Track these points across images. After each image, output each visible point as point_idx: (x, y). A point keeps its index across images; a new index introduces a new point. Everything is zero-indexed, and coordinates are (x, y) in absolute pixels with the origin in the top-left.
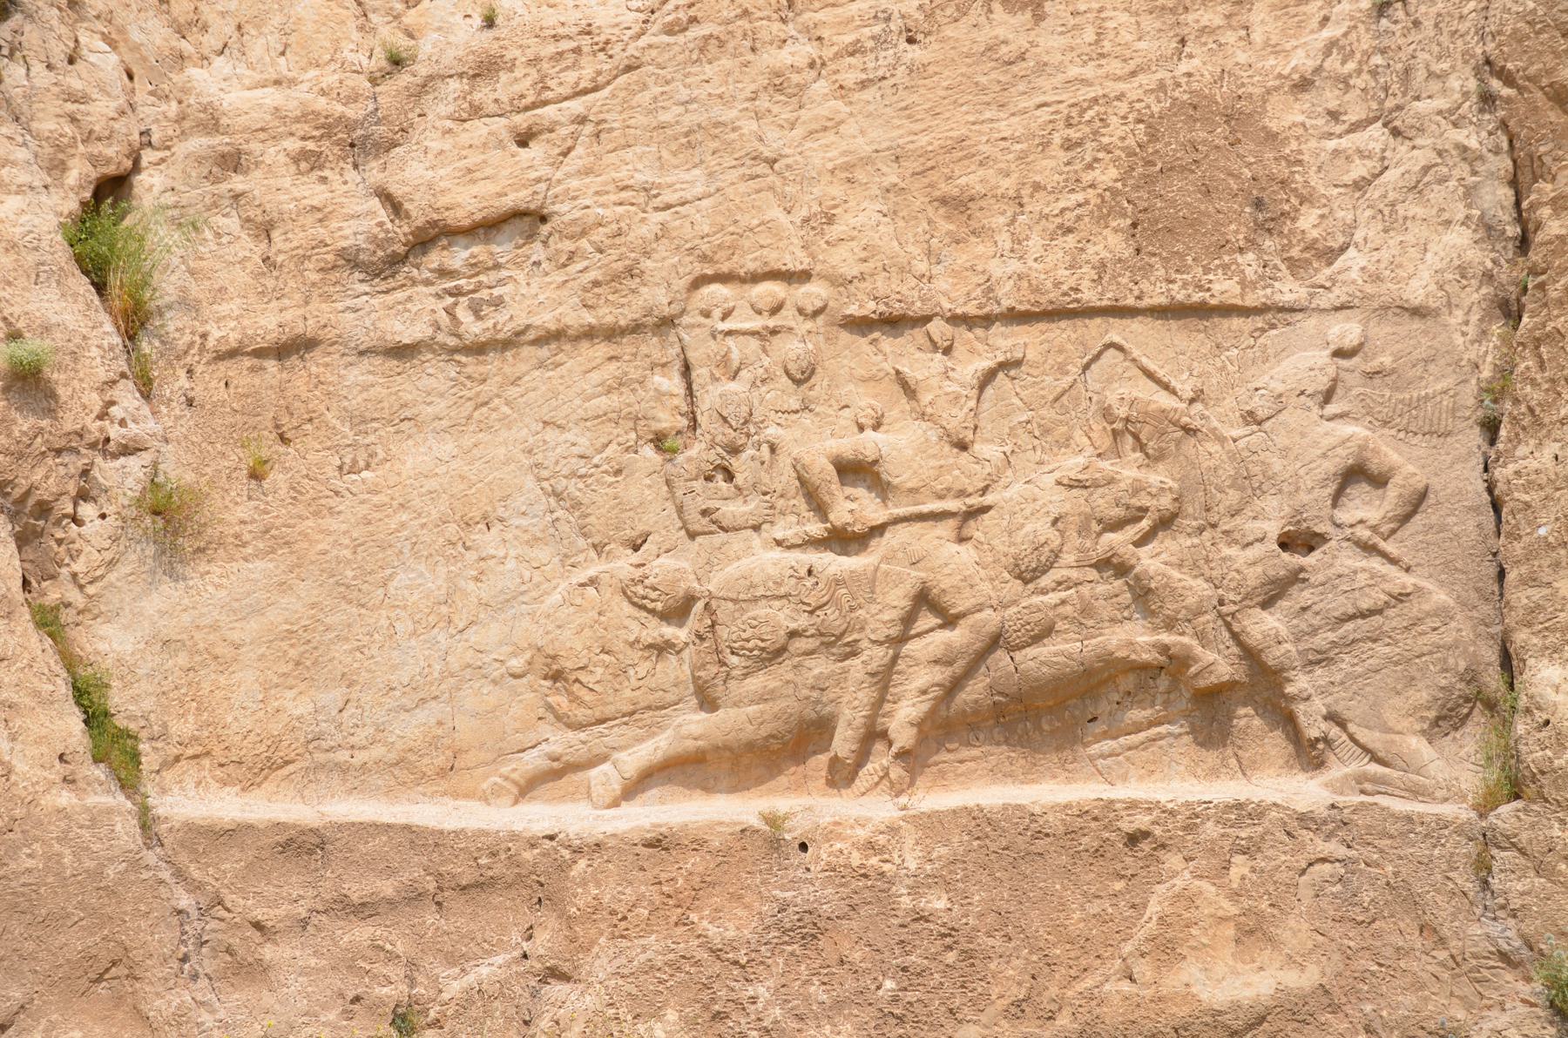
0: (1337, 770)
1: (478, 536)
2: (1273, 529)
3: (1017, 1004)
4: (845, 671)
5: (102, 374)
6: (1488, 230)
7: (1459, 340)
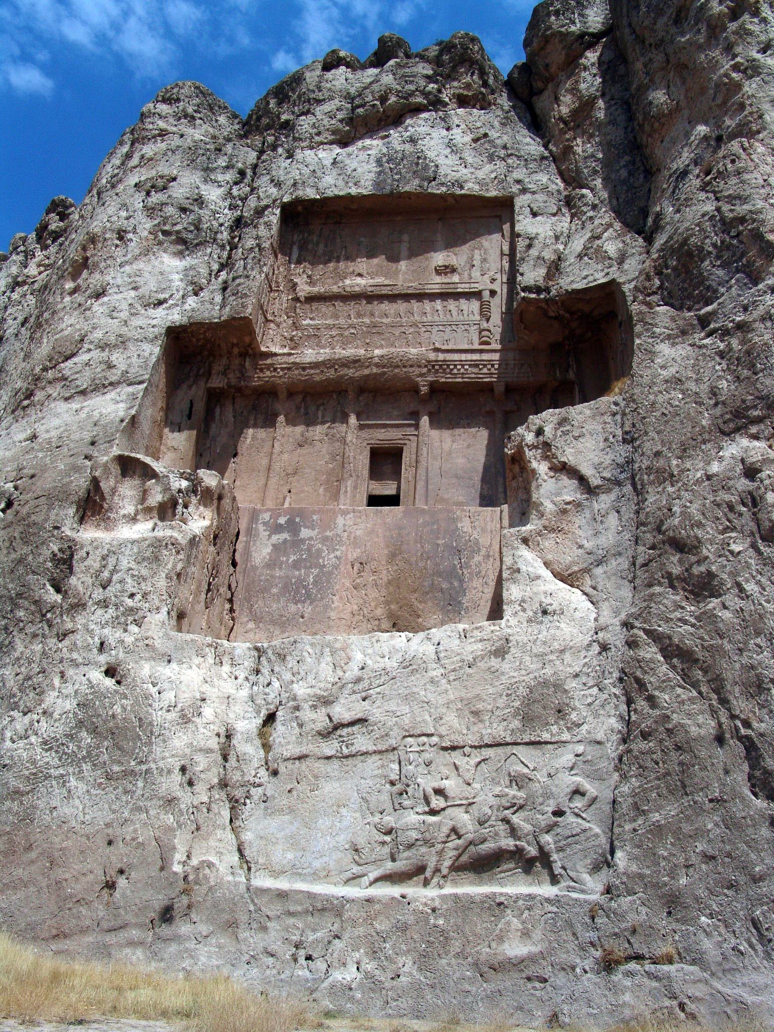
0: (563, 884)
2: (550, 809)
3: (458, 953)
5: (256, 766)
6: (621, 717)
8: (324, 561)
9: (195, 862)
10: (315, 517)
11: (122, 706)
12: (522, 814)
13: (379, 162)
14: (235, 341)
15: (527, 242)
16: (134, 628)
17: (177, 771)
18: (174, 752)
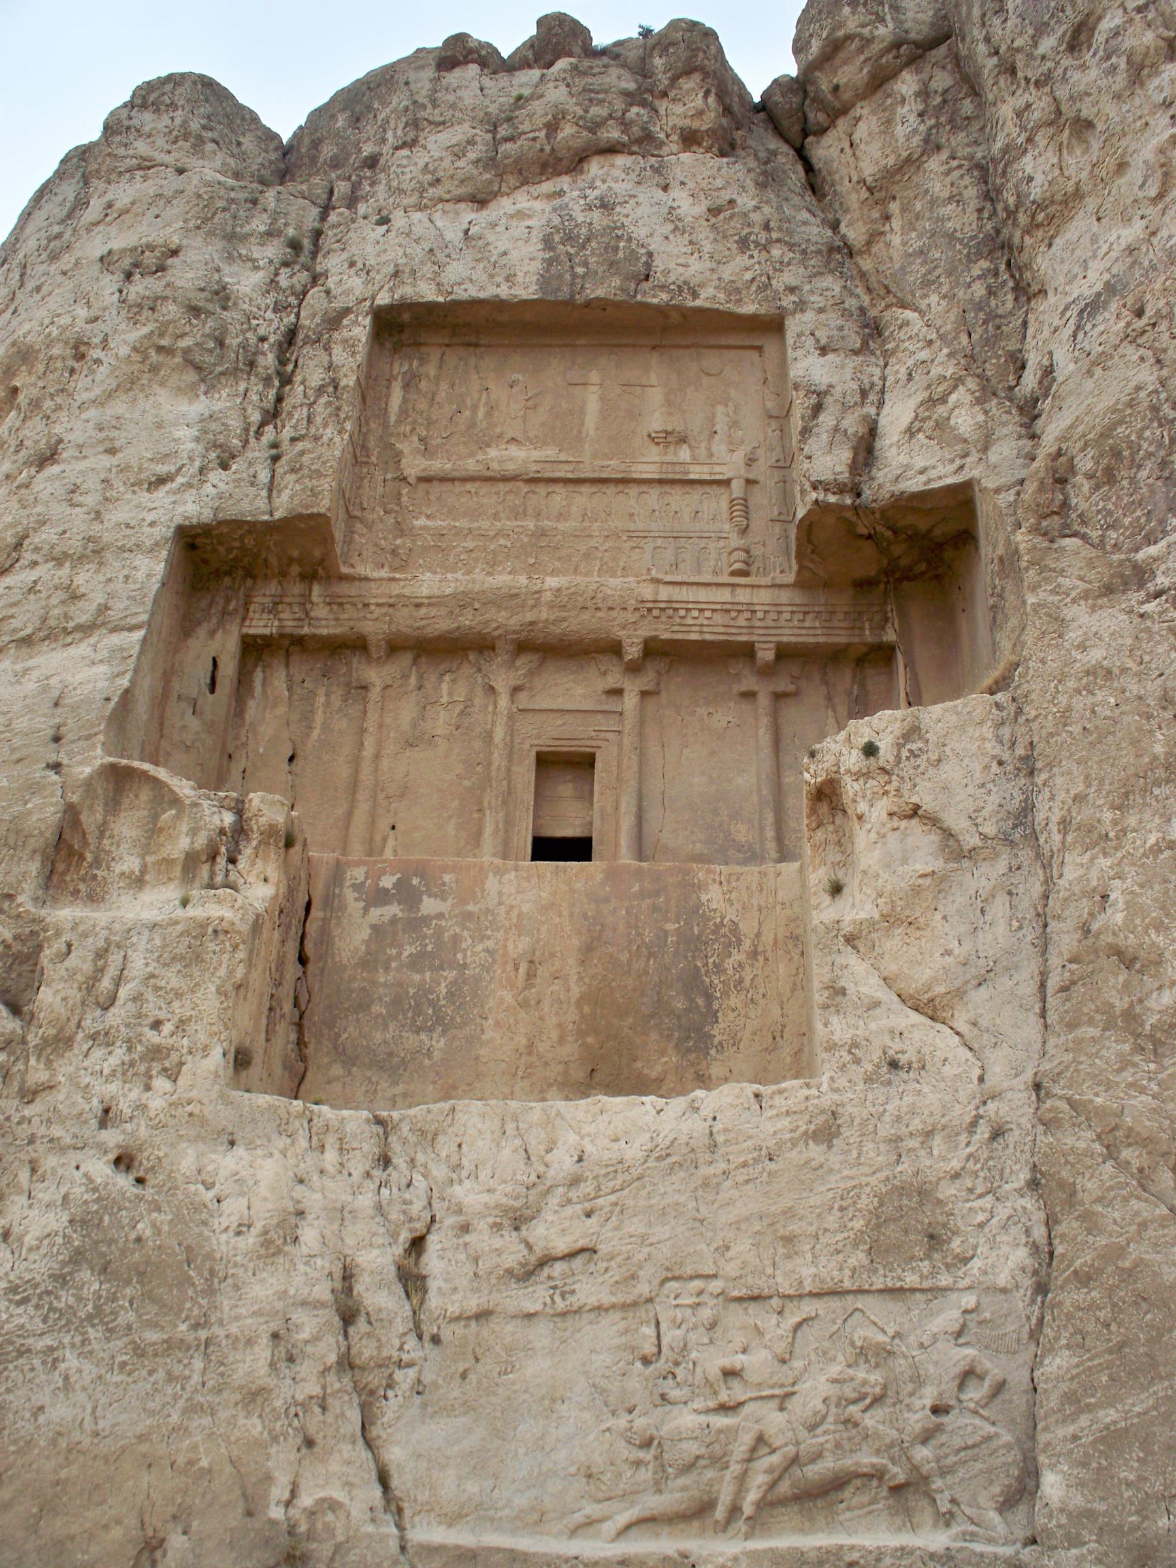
0: (955, 1529)
1: (558, 1406)
2: (928, 1402)
4: (722, 1478)
5: (401, 1330)
6: (1035, 1248)
7: (1021, 1304)
8: (465, 957)
9: (306, 1500)
10: (447, 878)
11: (154, 1224)
12: (879, 1413)
13: (548, 243)
14: (295, 554)
15: (813, 399)
16: (161, 1084)
17: (264, 1340)
18: (256, 1307)
